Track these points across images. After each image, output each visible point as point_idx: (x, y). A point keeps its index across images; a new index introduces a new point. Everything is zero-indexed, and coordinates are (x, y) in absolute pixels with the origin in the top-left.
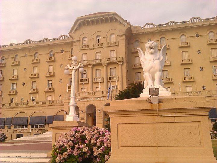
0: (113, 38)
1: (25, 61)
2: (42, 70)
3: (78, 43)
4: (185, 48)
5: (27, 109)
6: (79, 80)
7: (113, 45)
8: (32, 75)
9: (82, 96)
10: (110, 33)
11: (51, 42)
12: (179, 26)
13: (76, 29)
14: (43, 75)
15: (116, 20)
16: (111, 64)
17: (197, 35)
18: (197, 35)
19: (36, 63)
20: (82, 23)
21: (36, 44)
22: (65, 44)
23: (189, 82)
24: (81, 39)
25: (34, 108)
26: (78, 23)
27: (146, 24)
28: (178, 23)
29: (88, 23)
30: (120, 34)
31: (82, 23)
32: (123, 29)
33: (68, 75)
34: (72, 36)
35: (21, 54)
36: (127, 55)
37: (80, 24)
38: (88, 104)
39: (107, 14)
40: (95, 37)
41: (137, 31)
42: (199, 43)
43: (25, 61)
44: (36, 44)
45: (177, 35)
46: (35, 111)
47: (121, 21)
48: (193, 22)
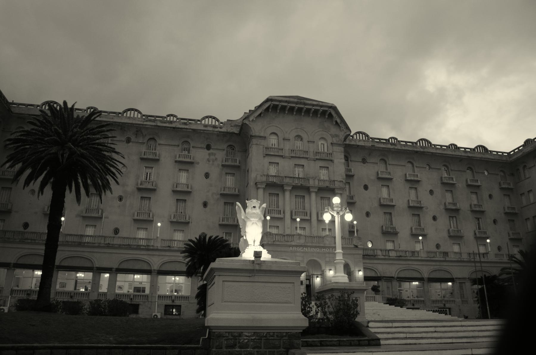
0: (322, 146)
1: (167, 153)
5: (150, 253)
9: (298, 241)
13: (260, 115)
14: (165, 189)
20: (271, 107)
21: (150, 121)
25: (168, 253)
26: (267, 105)
29: (283, 108)
30: (335, 141)
31: (276, 108)
33: (219, 196)
34: (250, 126)
36: (248, 171)
37: (267, 109)
43: (167, 153)
44: (150, 121)
46: (166, 259)
47: (339, 121)
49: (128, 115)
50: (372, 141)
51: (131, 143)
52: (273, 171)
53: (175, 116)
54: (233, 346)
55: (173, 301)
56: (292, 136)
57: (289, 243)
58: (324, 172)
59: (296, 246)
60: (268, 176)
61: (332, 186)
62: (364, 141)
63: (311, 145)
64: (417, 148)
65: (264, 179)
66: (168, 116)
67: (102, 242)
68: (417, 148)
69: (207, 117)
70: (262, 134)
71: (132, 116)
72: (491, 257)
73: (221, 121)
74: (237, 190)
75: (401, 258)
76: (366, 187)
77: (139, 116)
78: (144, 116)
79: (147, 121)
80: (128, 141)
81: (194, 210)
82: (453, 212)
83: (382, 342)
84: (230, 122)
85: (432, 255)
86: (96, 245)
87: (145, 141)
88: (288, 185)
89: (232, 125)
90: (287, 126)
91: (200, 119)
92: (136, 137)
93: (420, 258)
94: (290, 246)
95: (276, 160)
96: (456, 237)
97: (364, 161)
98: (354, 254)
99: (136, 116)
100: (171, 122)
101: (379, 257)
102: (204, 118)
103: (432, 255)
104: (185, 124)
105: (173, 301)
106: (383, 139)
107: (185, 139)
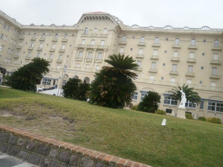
0: (105, 32)
2: (57, 47)
3: (81, 32)
4: (156, 47)
6: (76, 58)
8: (51, 49)
10: (85, 27)
11: (67, 28)
12: (156, 30)
15: (110, 19)
17: (167, 39)
18: (205, 41)
19: (54, 42)
23: (153, 73)
24: (84, 29)
26: (84, 17)
27: (134, 25)
28: (156, 28)
30: (110, 29)
32: (113, 26)
35: (46, 34)
37: (85, 18)
38: (85, 76)
41: (126, 29)
42: (166, 45)
48: (137, 28)
49: (134, 28)
52: (84, 43)
56: (93, 29)
58: (103, 42)
71: (137, 28)
76: (132, 49)
81: (159, 67)
82: (175, 62)
95: (93, 38)
96: (174, 75)
97: (133, 38)
107: (56, 33)
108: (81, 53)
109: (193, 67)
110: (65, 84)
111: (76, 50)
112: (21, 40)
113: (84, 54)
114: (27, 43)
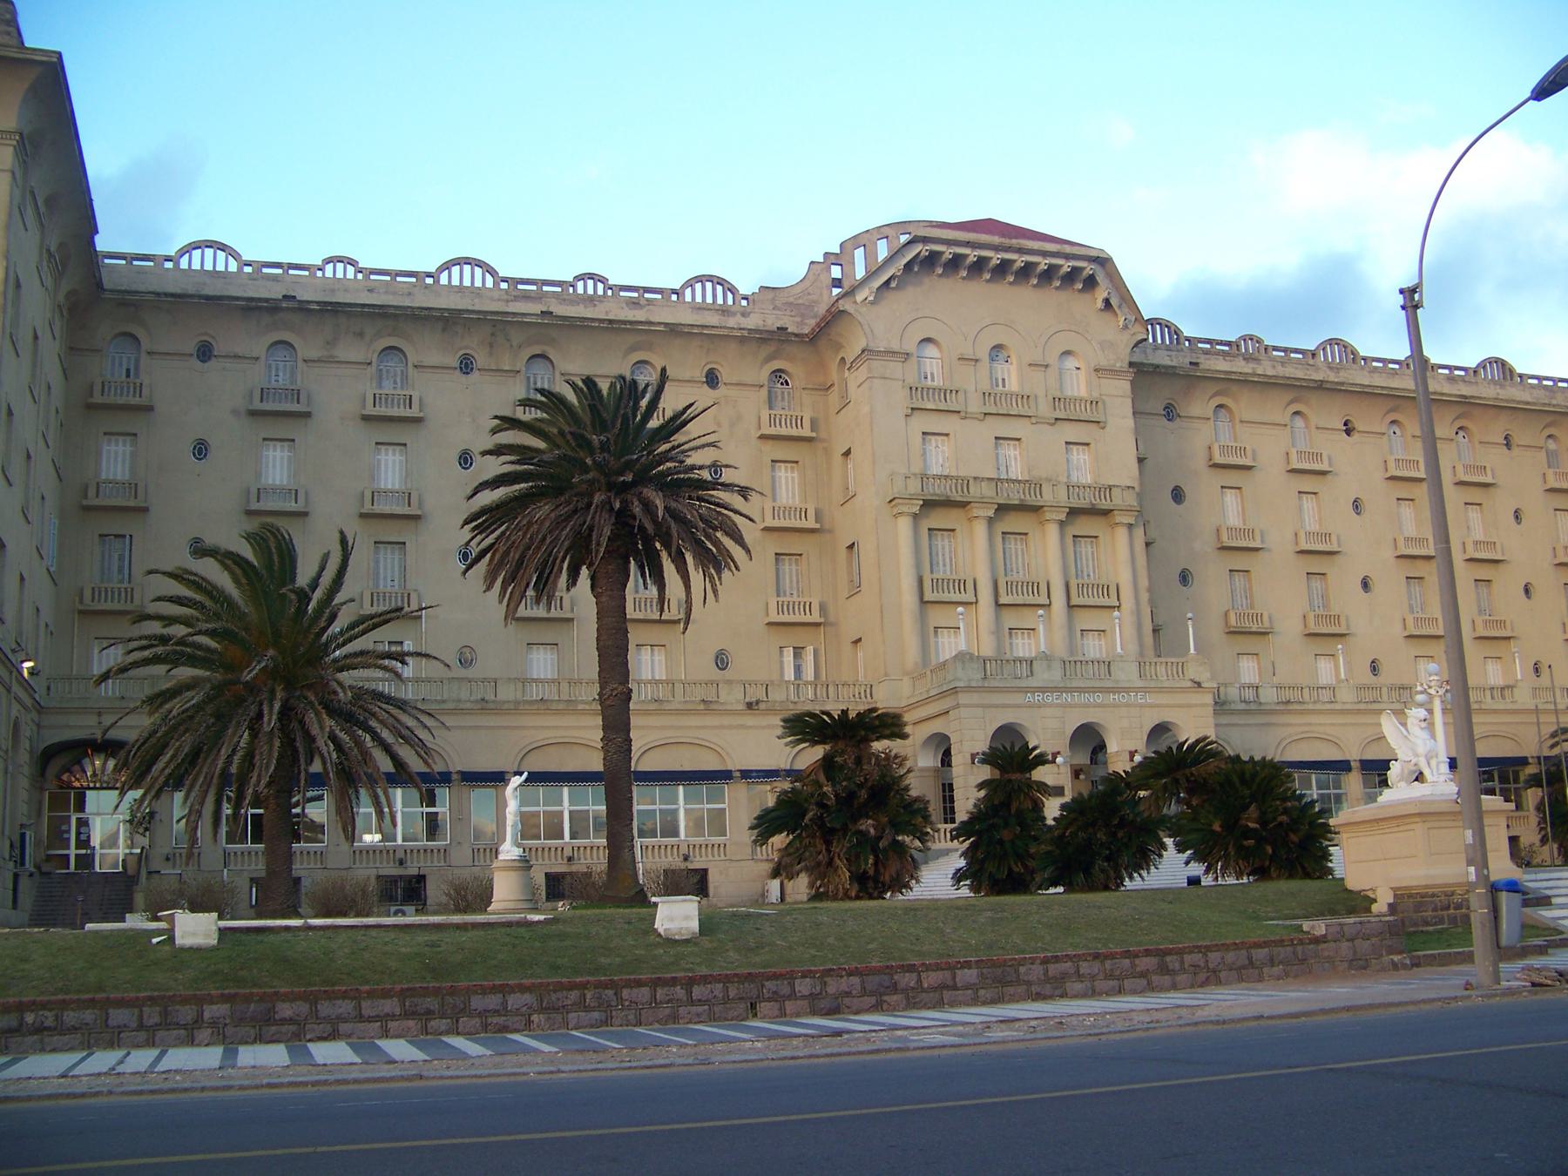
4: (1311, 474)
7: (1078, 417)
9: (1046, 676)
12: (1283, 364)
13: (887, 282)
16: (1086, 513)
21: (526, 296)
22: (742, 340)
28: (1276, 349)
30: (1104, 363)
35: (427, 350)
37: (908, 266)
39: (1068, 249)
40: (983, 352)
45: (1275, 408)
50: (1191, 349)
51: (476, 374)
53: (603, 280)
54: (1448, 908)
55: (686, 858)
57: (1024, 683)
58: (1079, 456)
59: (1043, 690)
60: (924, 477)
61: (1104, 504)
62: (1168, 349)
63: (1038, 375)
64: (1317, 369)
65: (914, 487)
66: (582, 277)
67: (464, 695)
68: (1317, 369)
69: (701, 279)
70: (895, 347)
72: (1523, 698)
73: (744, 289)
74: (811, 514)
75: (1291, 707)
77: (490, 282)
78: (504, 280)
79: (516, 299)
80: (466, 366)
83: (1554, 901)
84: (770, 295)
85: (1370, 695)
86: (450, 705)
87: (520, 364)
88: (983, 502)
89: (778, 303)
90: (961, 311)
91: (677, 287)
92: (491, 354)
93: (1338, 707)
94: (1026, 690)
98: (1189, 706)
99: (478, 283)
100: (591, 300)
101: (1233, 707)
102: (690, 284)
103: (1370, 695)
104: (634, 303)
105: (686, 858)
106: (1221, 343)
108: (942, 542)
109: (1495, 586)
110: (1324, 798)
111: (904, 526)
112: (126, 412)
113: (971, 550)
114: (201, 449)
